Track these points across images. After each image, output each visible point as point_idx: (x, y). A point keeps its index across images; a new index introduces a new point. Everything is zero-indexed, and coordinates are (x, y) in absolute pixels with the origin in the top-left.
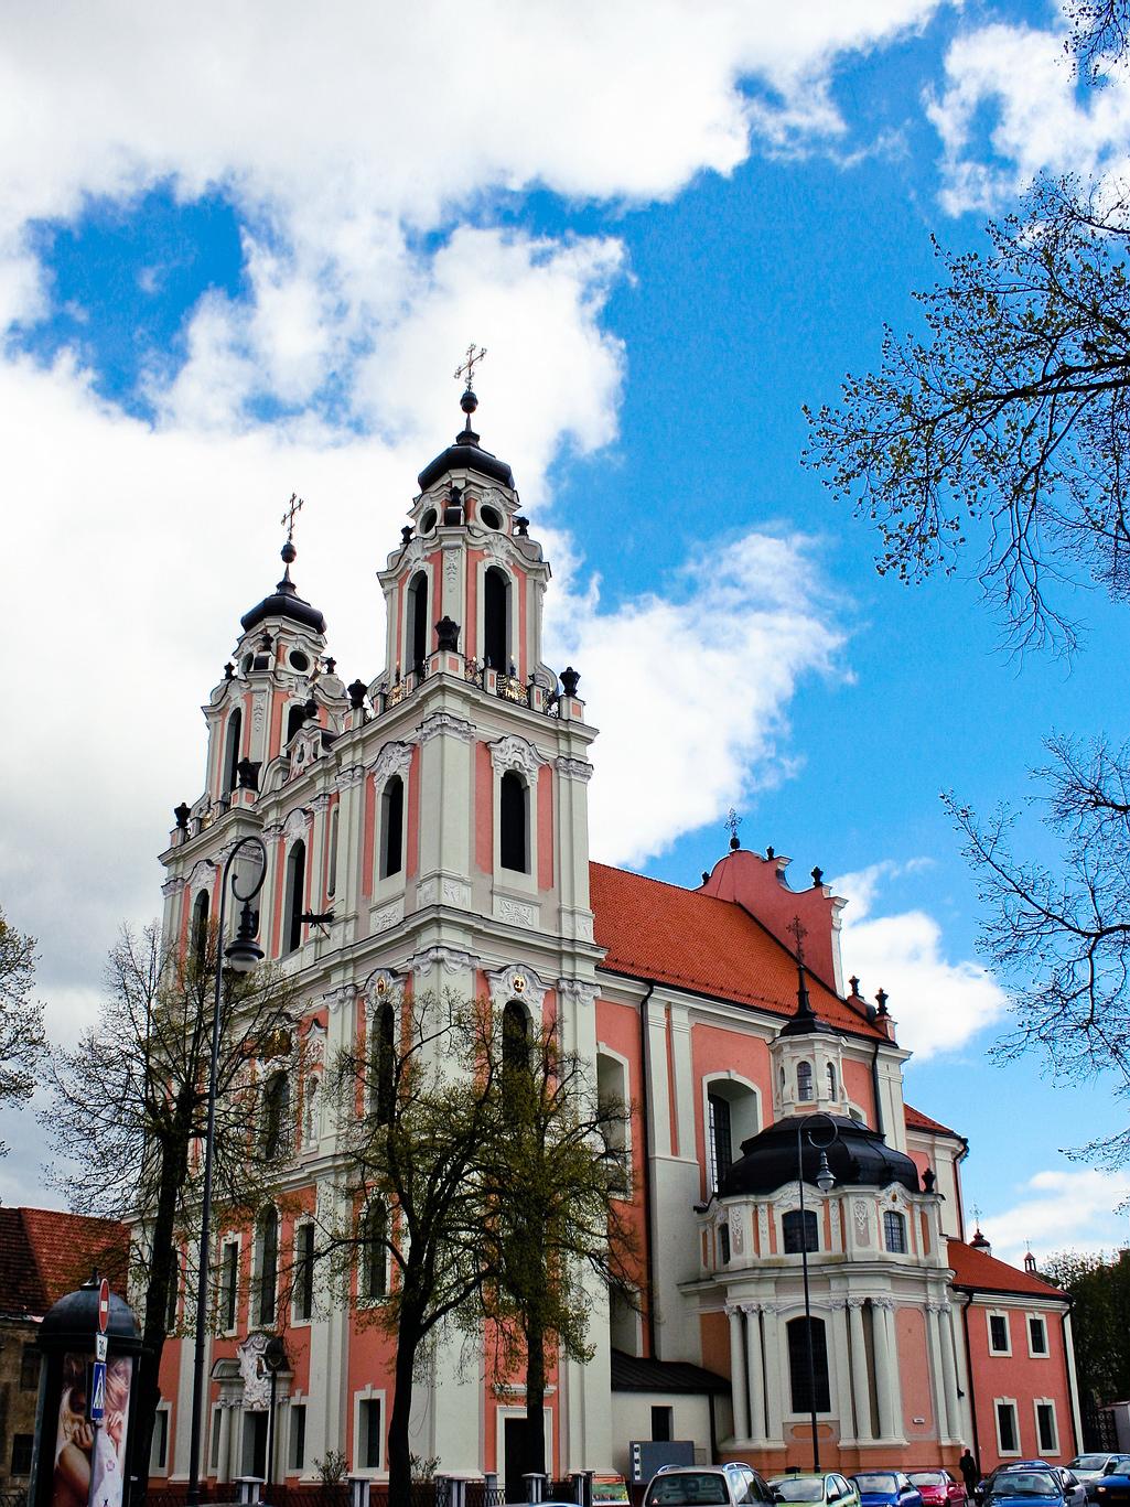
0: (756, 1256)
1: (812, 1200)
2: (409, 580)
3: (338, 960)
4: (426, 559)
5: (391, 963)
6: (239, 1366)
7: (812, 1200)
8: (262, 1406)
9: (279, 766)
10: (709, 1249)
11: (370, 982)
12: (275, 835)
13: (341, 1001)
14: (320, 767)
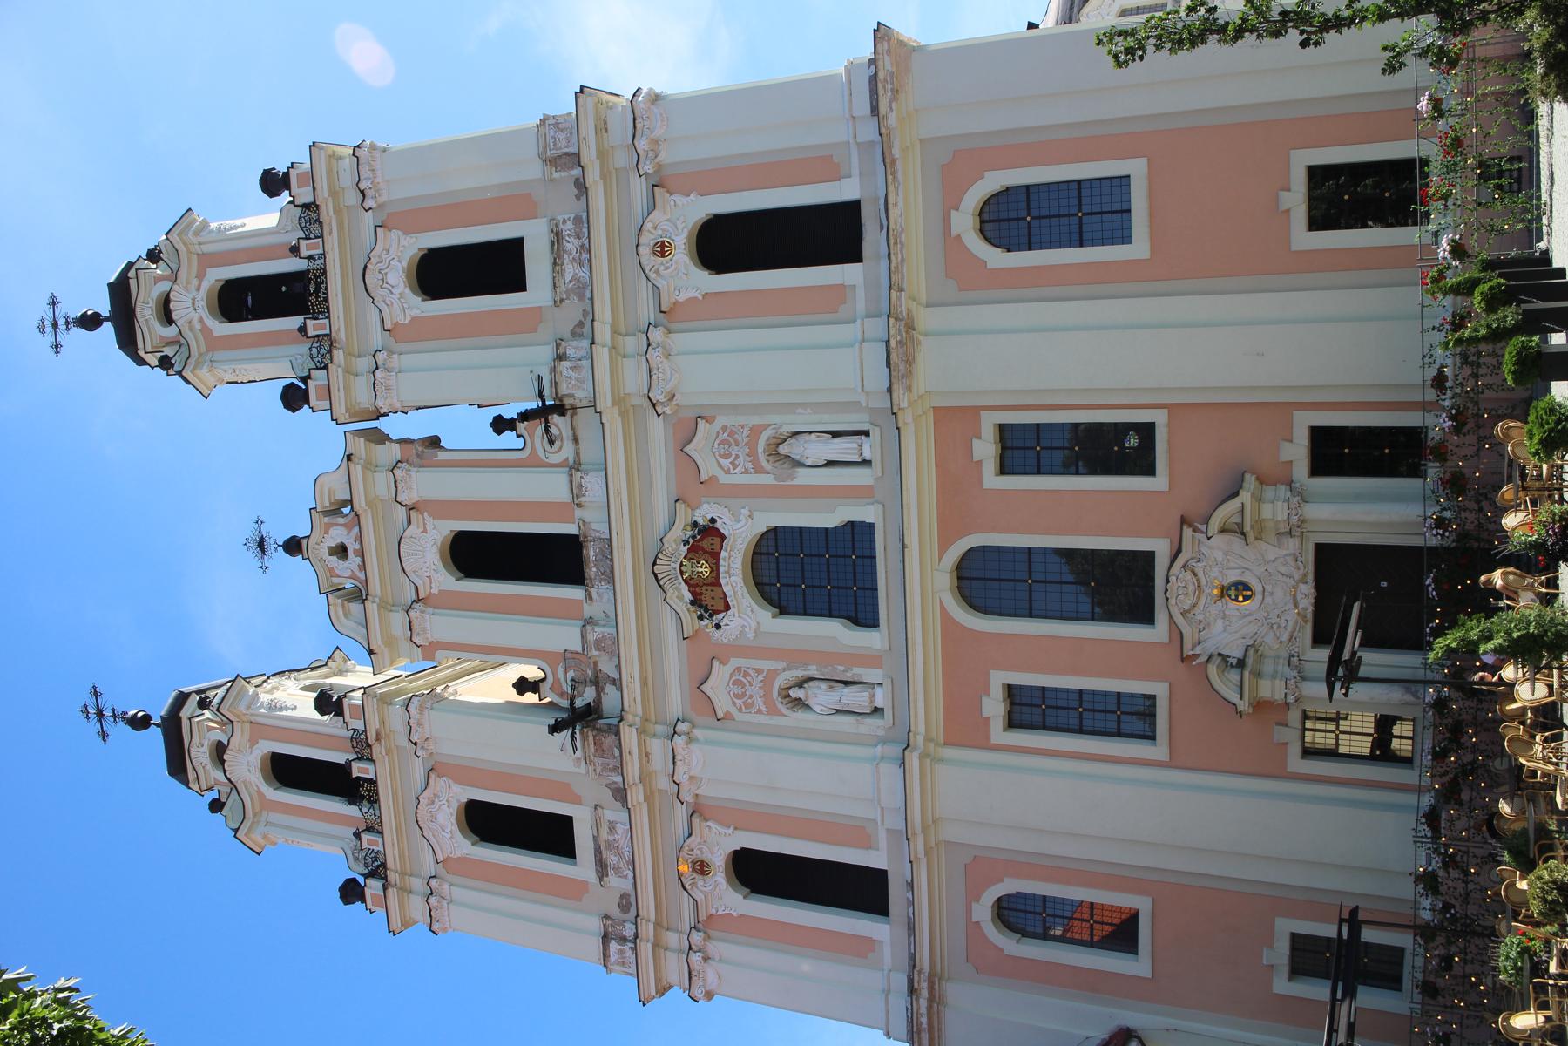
11: (652, 275)
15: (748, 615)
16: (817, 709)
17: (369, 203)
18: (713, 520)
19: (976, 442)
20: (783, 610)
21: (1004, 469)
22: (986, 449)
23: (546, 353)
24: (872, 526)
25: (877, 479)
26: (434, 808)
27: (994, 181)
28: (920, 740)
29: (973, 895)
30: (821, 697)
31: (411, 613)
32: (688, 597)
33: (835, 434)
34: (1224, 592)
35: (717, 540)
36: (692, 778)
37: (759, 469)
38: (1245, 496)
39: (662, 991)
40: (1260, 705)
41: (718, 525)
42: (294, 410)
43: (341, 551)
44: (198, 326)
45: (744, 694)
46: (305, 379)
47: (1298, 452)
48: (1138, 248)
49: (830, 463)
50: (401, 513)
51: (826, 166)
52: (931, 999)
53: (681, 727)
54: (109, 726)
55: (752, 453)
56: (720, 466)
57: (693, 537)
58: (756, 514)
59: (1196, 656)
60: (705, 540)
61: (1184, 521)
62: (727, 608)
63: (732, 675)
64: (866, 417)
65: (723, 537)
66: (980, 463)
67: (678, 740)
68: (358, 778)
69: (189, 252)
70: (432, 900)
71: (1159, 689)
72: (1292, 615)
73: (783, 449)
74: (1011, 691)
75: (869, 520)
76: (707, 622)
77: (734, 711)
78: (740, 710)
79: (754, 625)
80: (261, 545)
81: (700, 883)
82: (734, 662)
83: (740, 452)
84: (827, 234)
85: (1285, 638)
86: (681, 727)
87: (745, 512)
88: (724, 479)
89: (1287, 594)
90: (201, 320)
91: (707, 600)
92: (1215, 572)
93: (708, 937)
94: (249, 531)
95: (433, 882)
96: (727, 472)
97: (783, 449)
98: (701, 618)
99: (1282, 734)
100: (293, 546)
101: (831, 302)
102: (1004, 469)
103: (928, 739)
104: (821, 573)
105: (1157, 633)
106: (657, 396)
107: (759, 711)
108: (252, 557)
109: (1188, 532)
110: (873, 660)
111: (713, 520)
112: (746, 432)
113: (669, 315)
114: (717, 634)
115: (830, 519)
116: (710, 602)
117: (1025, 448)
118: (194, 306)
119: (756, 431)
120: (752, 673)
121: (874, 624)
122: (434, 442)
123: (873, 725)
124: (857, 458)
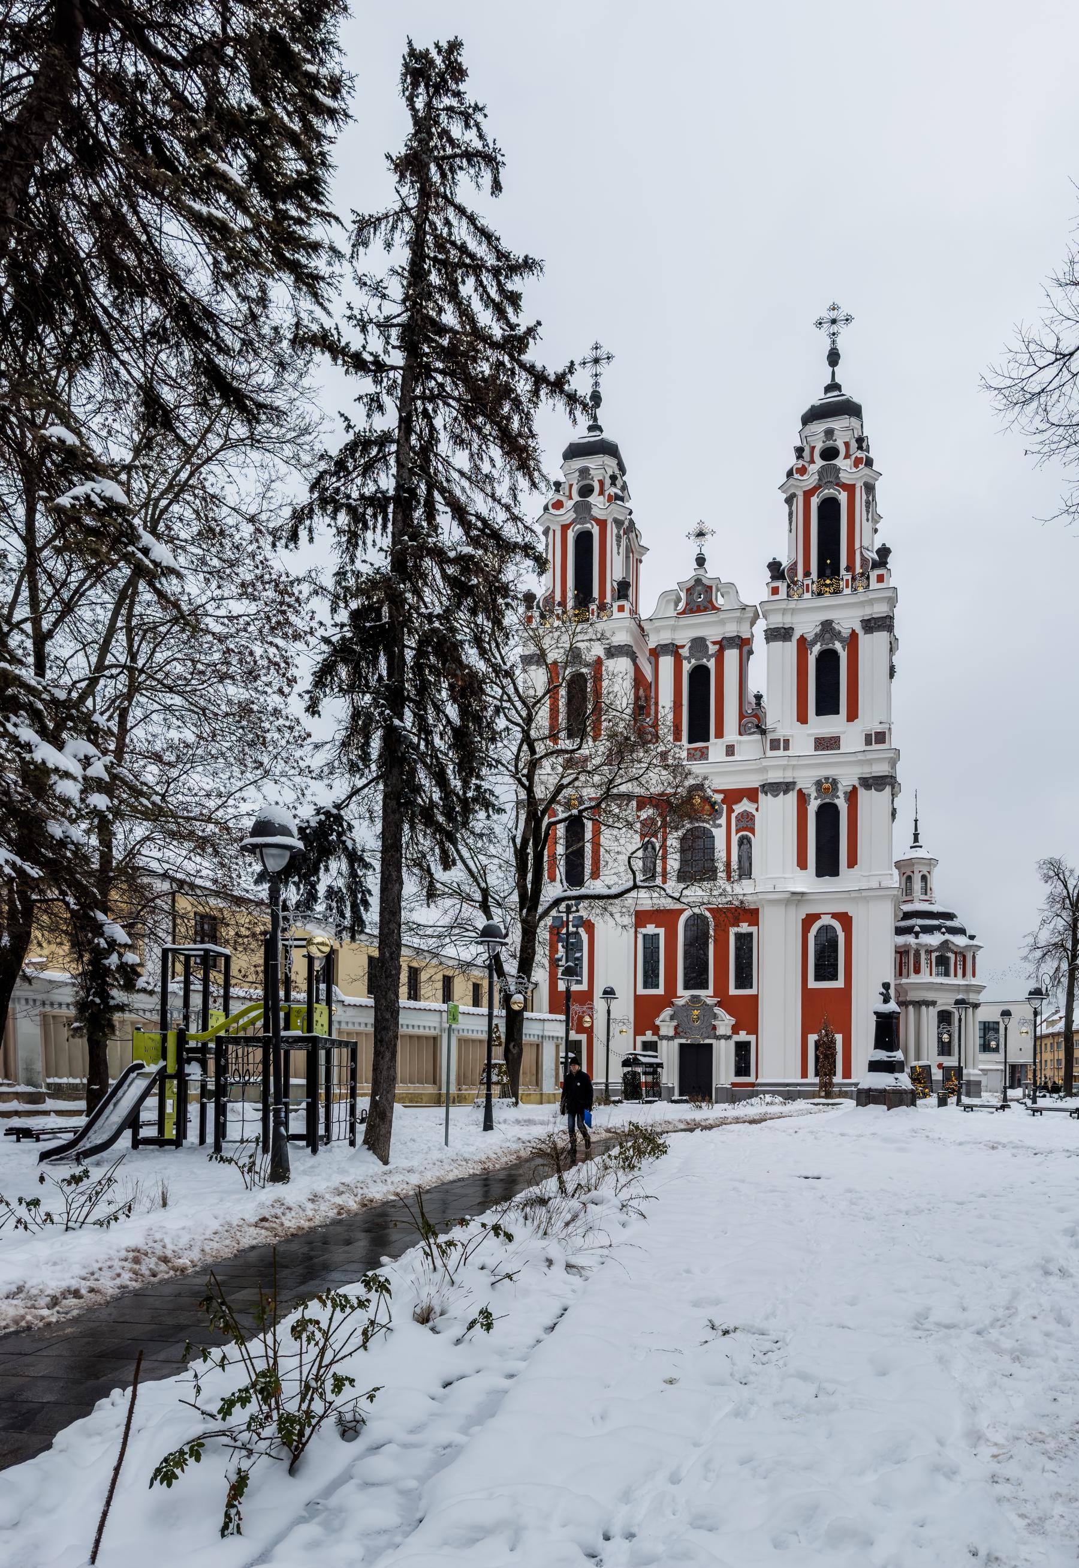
22: (744, 928)
80: (701, 534)
83: (743, 824)
88: (734, 816)
94: (708, 527)
100: (701, 561)
108: (693, 528)
117: (745, 942)
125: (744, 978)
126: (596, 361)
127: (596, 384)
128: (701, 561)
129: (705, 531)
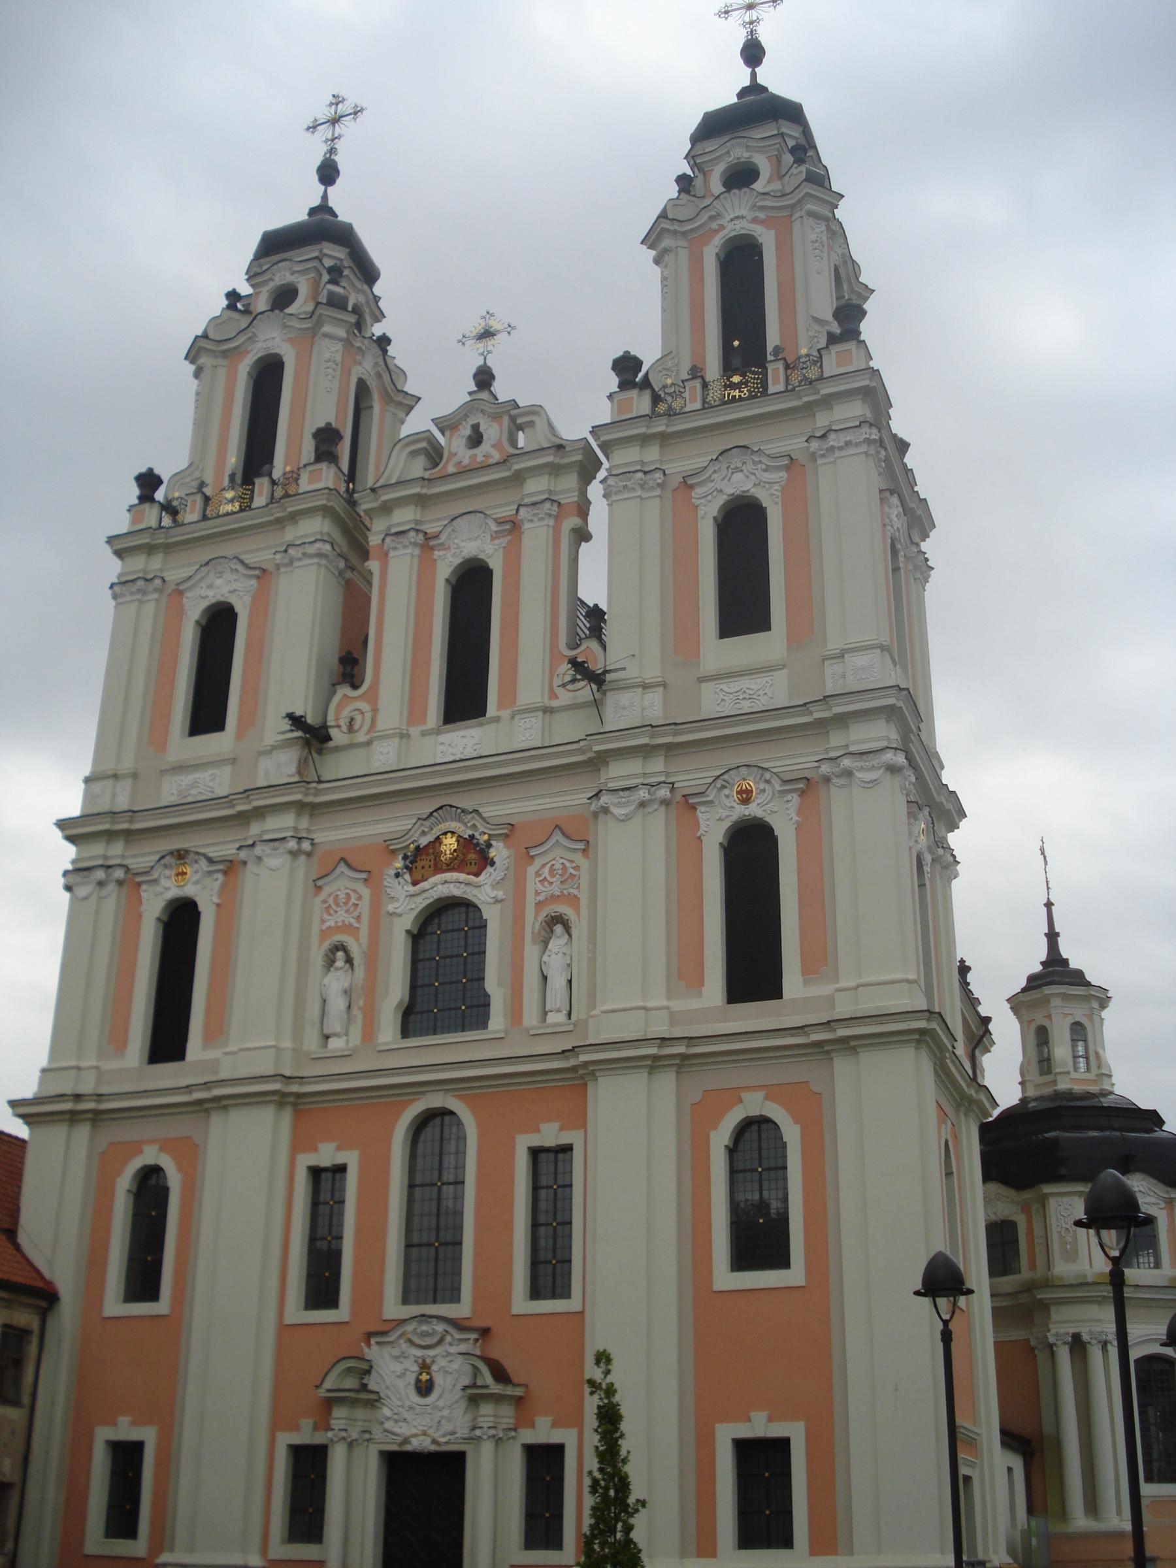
0: (1088, 1267)
1: (1153, 1200)
2: (717, 241)
3: (645, 740)
4: (755, 220)
5: (769, 760)
6: (368, 1372)
7: (1153, 1200)
8: (434, 1442)
9: (424, 445)
10: (1037, 1248)
11: (719, 784)
12: (415, 544)
13: (642, 804)
14: (550, 459)
15: (406, 901)
16: (326, 981)
17: (814, 445)
18: (492, 863)
19: (555, 1126)
20: (417, 937)
21: (536, 1153)
22: (550, 1135)
23: (652, 673)
24: (483, 1024)
25: (527, 1030)
26: (228, 576)
27: (791, 1133)
28: (295, 1088)
29: (165, 1146)
30: (336, 982)
31: (412, 534)
32: (424, 841)
33: (570, 982)
34: (425, 1367)
35: (475, 869)
36: (259, 859)
37: (539, 905)
38: (495, 1388)
39: (70, 839)
40: (329, 1404)
41: (489, 869)
42: (614, 368)
43: (476, 439)
44: (714, 225)
45: (338, 905)
46: (646, 384)
47: (543, 1432)
48: (725, 1278)
49: (545, 978)
50: (509, 511)
51: (818, 962)
52: (72, 1113)
53: (306, 845)
54: (324, 132)
55: (553, 898)
56: (544, 865)
57: (478, 844)
58: (498, 906)
59: (369, 1345)
60: (474, 856)
61: (485, 1332)
62: (415, 883)
63: (354, 891)
64: (583, 1016)
65: (477, 875)
66: (538, 1130)
67: (292, 844)
68: (253, 484)
69: (792, 206)
70: (141, 583)
71: (342, 1313)
72: (404, 1430)
73: (559, 929)
74: (341, 1169)
75: (491, 1023)
76: (399, 864)
77: (323, 895)
78: (325, 902)
79: (398, 911)
80: (487, 334)
81: (168, 872)
82: (366, 892)
83: (556, 889)
84: (753, 969)
85: (389, 1425)
86: (306, 845)
87: (500, 894)
88: (531, 870)
89: (423, 1425)
90: (722, 227)
91: (421, 860)
92: (442, 1362)
93: (120, 883)
95: (158, 582)
96: (538, 874)
97: (559, 929)
98: (405, 858)
99: (307, 1424)
100: (484, 378)
101: (688, 974)
102: (536, 1153)
103: (298, 1095)
104: (446, 974)
105: (393, 1308)
106: (605, 799)
107: (323, 921)
108: (475, 325)
109: (474, 1336)
110: (369, 1034)
111: (492, 863)
112: (575, 892)
113: (687, 805)
114: (392, 872)
115: (492, 984)
116: (419, 864)
118: (738, 216)
119: (574, 901)
120: (356, 914)
121: (405, 1032)
122: (582, 535)
123: (311, 1042)
124: (548, 1008)
125: (551, 1271)
126: (334, 121)
127: (332, 151)
128: (484, 378)
129: (495, 325)
